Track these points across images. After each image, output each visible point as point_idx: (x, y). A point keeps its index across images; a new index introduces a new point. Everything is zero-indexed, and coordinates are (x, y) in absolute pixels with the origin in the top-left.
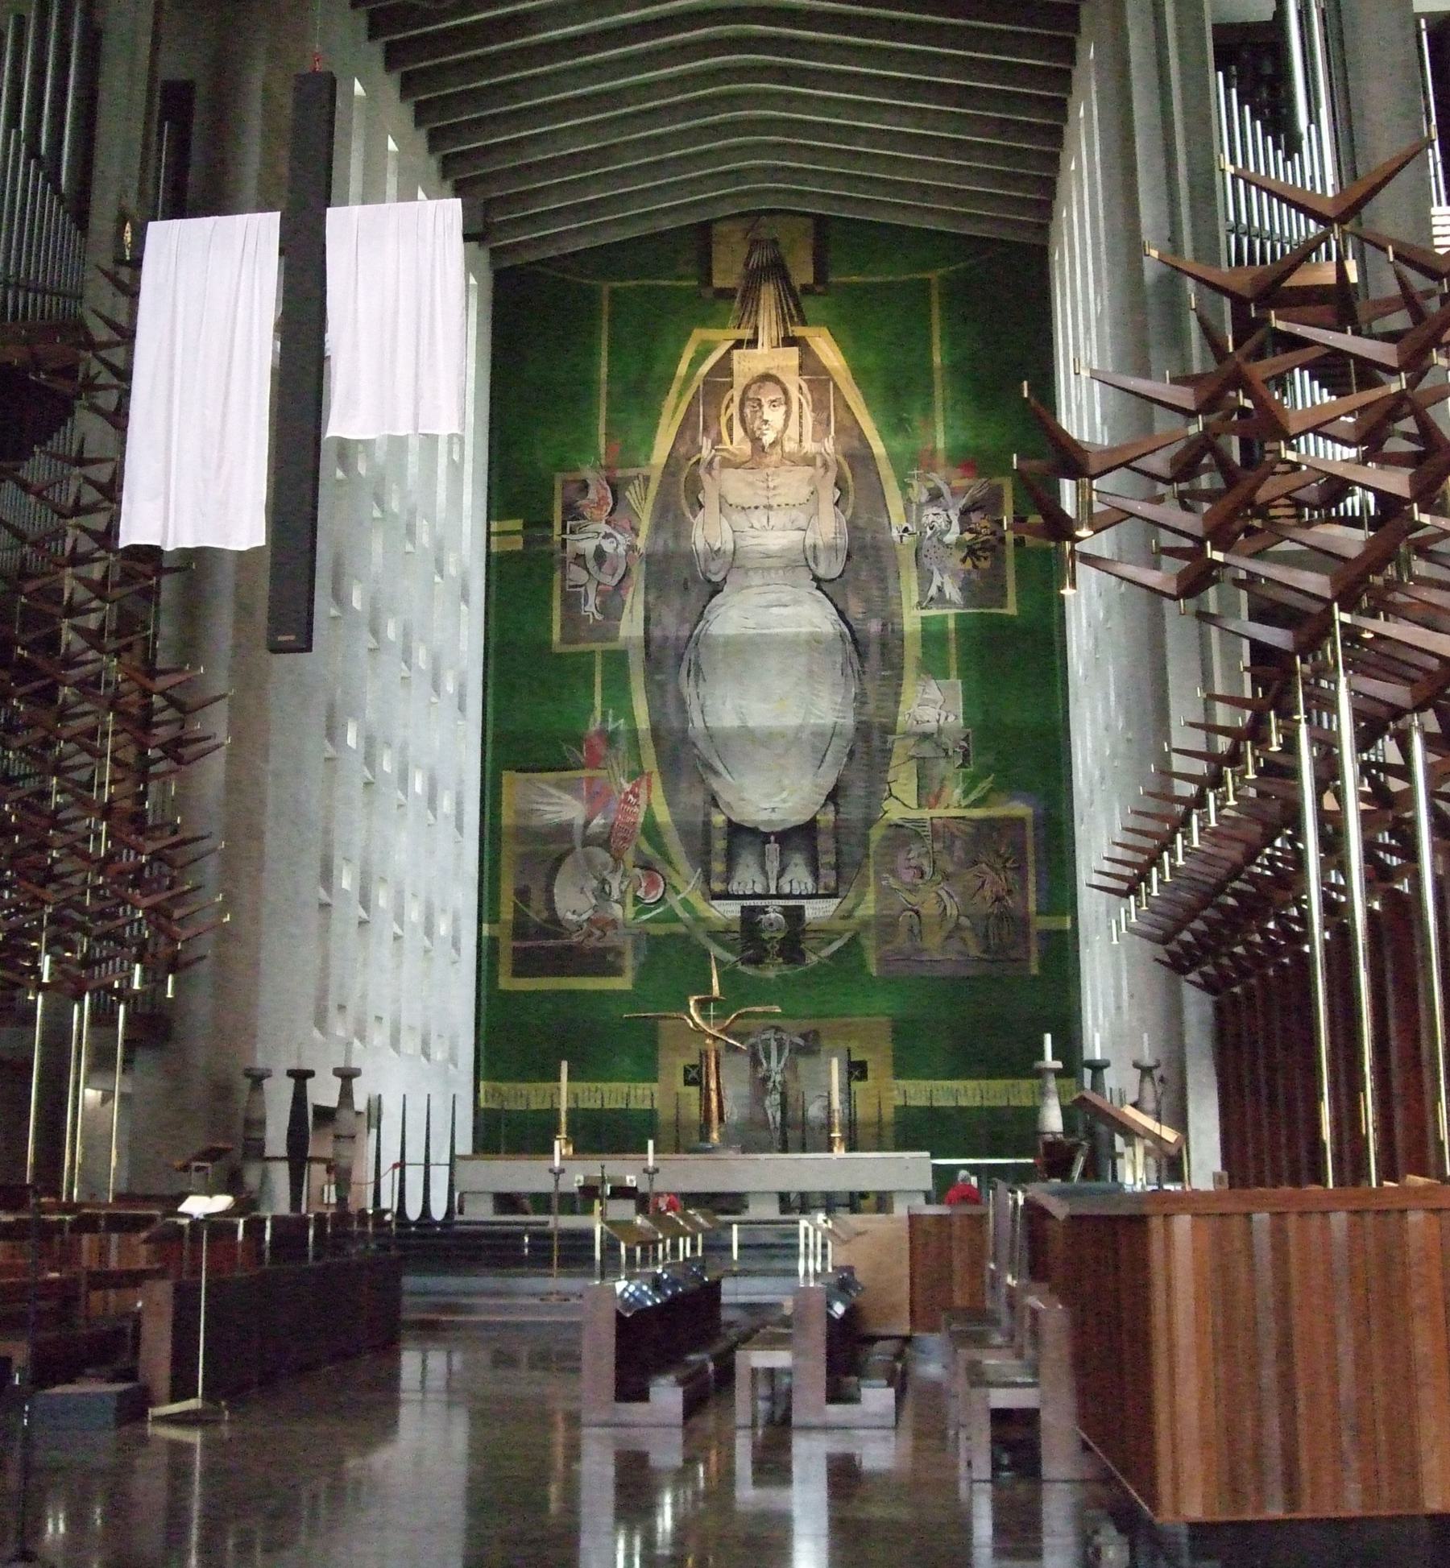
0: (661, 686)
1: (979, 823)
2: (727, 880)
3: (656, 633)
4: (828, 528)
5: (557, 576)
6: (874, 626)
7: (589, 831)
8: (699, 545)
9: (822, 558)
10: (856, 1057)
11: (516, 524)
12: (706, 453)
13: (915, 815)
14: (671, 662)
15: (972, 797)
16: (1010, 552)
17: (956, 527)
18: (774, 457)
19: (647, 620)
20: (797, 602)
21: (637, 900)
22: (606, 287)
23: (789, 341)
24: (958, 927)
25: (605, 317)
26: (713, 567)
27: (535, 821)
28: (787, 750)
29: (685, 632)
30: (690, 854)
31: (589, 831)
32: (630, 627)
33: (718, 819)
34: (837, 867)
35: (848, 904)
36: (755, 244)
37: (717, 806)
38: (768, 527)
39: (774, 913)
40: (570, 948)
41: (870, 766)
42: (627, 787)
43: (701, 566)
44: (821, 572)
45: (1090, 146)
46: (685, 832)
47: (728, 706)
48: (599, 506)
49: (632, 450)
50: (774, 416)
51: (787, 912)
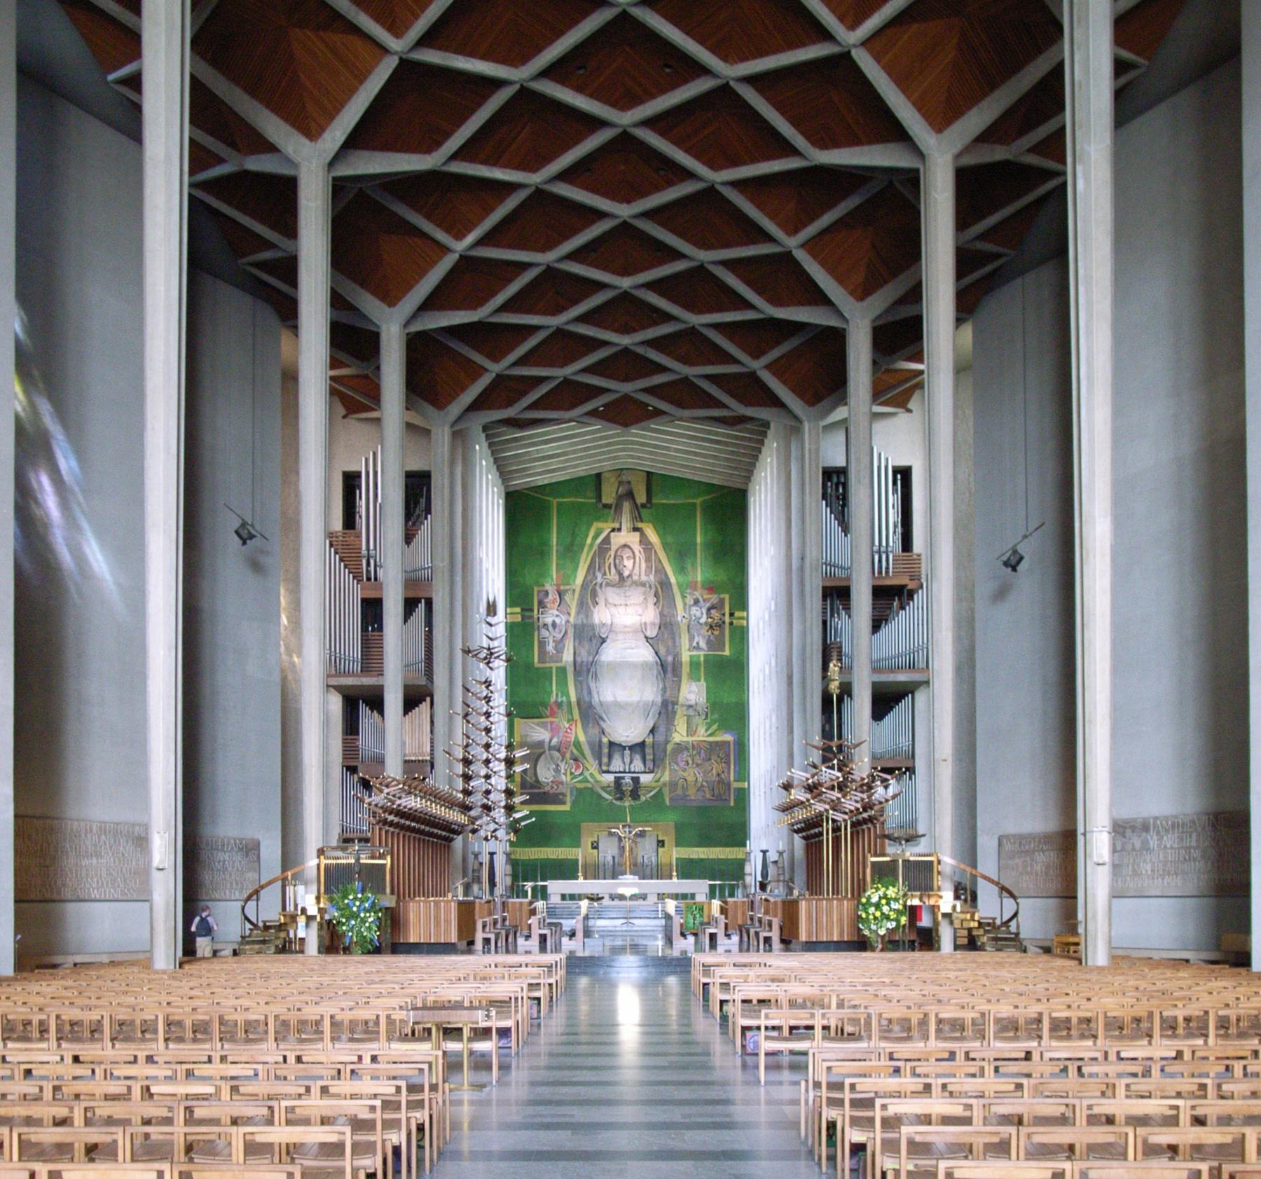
0: (581, 683)
1: (710, 743)
2: (609, 765)
3: (578, 659)
4: (650, 615)
5: (536, 633)
6: (670, 659)
7: (552, 744)
9: (648, 628)
10: (660, 838)
11: (518, 610)
12: (599, 580)
13: (685, 739)
15: (709, 732)
16: (727, 625)
17: (705, 616)
18: (629, 582)
19: (575, 653)
20: (637, 647)
21: (572, 773)
22: (554, 502)
23: (636, 529)
24: (702, 785)
25: (555, 510)
26: (603, 631)
27: (529, 740)
28: (633, 712)
29: (591, 659)
31: (552, 744)
32: (568, 657)
33: (605, 740)
34: (654, 761)
35: (658, 776)
36: (620, 483)
37: (604, 733)
39: (627, 779)
40: (544, 793)
41: (667, 718)
42: (567, 726)
43: (597, 630)
44: (649, 634)
46: (590, 744)
47: (609, 693)
48: (553, 603)
49: (566, 579)
50: (628, 563)
51: (633, 778)
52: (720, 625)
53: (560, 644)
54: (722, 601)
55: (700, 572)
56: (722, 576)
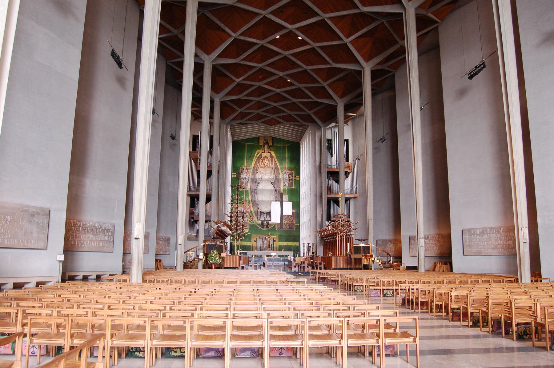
3: (252, 188)
4: (273, 176)
6: (278, 188)
8: (257, 177)
11: (235, 173)
12: (258, 166)
14: (254, 192)
20: (269, 185)
23: (269, 152)
30: (255, 215)
32: (249, 187)
33: (259, 211)
36: (265, 140)
38: (266, 176)
39: (265, 222)
45: (309, 139)
46: (255, 212)
49: (249, 165)
50: (267, 162)
52: (292, 180)
53: (247, 183)
54: (292, 173)
55: (286, 165)
56: (293, 166)
